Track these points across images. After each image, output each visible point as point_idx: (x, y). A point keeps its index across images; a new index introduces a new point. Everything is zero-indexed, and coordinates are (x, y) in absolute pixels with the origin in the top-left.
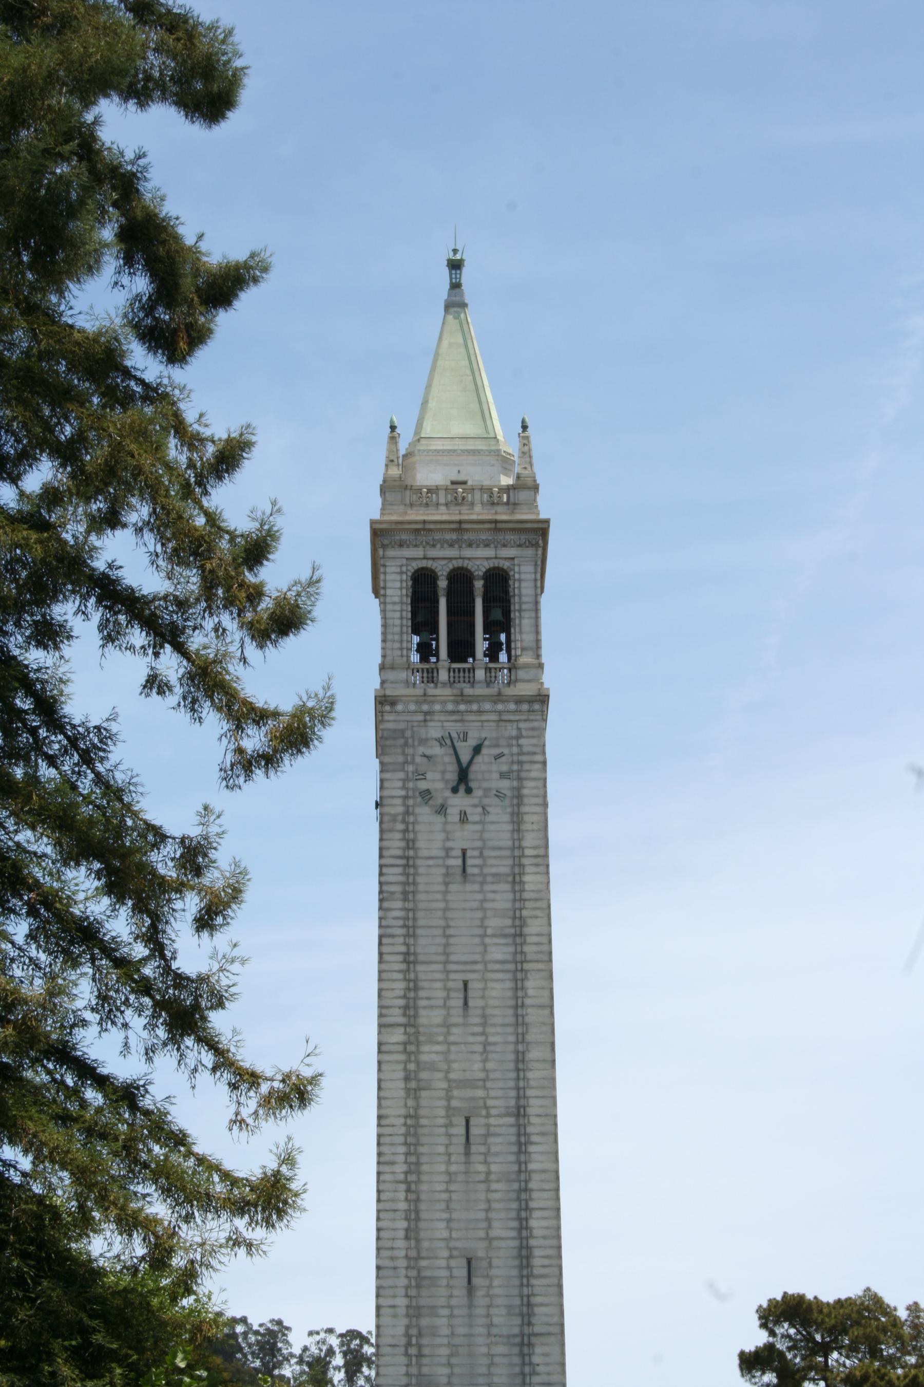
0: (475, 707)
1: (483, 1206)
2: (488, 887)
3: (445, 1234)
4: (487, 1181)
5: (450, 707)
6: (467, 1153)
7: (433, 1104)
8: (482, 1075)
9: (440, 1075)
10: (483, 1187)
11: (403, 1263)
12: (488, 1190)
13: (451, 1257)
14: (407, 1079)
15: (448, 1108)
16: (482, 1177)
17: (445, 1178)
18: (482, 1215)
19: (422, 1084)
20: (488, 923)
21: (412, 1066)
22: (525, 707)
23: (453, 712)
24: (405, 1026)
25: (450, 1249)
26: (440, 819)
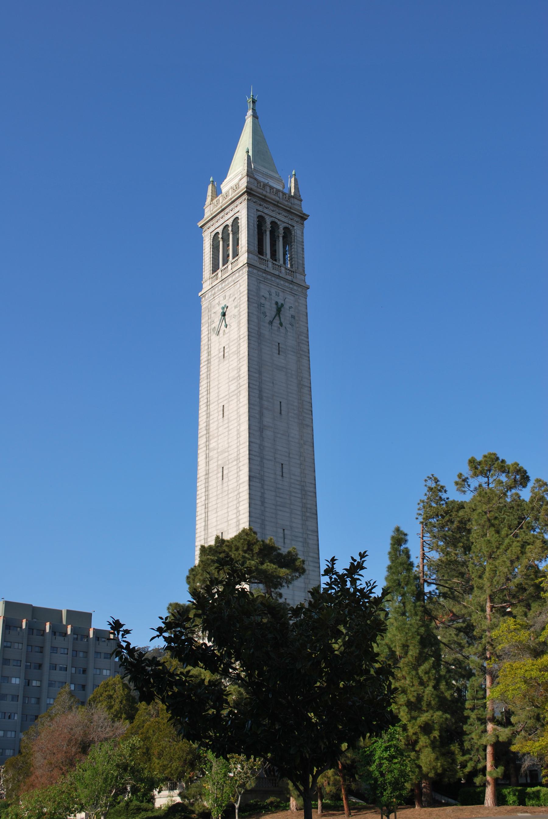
1: (226, 506)
2: (231, 360)
4: (228, 494)
5: (220, 287)
6: (222, 484)
8: (227, 446)
15: (218, 465)
16: (226, 493)
18: (226, 511)
20: (230, 376)
25: (217, 530)
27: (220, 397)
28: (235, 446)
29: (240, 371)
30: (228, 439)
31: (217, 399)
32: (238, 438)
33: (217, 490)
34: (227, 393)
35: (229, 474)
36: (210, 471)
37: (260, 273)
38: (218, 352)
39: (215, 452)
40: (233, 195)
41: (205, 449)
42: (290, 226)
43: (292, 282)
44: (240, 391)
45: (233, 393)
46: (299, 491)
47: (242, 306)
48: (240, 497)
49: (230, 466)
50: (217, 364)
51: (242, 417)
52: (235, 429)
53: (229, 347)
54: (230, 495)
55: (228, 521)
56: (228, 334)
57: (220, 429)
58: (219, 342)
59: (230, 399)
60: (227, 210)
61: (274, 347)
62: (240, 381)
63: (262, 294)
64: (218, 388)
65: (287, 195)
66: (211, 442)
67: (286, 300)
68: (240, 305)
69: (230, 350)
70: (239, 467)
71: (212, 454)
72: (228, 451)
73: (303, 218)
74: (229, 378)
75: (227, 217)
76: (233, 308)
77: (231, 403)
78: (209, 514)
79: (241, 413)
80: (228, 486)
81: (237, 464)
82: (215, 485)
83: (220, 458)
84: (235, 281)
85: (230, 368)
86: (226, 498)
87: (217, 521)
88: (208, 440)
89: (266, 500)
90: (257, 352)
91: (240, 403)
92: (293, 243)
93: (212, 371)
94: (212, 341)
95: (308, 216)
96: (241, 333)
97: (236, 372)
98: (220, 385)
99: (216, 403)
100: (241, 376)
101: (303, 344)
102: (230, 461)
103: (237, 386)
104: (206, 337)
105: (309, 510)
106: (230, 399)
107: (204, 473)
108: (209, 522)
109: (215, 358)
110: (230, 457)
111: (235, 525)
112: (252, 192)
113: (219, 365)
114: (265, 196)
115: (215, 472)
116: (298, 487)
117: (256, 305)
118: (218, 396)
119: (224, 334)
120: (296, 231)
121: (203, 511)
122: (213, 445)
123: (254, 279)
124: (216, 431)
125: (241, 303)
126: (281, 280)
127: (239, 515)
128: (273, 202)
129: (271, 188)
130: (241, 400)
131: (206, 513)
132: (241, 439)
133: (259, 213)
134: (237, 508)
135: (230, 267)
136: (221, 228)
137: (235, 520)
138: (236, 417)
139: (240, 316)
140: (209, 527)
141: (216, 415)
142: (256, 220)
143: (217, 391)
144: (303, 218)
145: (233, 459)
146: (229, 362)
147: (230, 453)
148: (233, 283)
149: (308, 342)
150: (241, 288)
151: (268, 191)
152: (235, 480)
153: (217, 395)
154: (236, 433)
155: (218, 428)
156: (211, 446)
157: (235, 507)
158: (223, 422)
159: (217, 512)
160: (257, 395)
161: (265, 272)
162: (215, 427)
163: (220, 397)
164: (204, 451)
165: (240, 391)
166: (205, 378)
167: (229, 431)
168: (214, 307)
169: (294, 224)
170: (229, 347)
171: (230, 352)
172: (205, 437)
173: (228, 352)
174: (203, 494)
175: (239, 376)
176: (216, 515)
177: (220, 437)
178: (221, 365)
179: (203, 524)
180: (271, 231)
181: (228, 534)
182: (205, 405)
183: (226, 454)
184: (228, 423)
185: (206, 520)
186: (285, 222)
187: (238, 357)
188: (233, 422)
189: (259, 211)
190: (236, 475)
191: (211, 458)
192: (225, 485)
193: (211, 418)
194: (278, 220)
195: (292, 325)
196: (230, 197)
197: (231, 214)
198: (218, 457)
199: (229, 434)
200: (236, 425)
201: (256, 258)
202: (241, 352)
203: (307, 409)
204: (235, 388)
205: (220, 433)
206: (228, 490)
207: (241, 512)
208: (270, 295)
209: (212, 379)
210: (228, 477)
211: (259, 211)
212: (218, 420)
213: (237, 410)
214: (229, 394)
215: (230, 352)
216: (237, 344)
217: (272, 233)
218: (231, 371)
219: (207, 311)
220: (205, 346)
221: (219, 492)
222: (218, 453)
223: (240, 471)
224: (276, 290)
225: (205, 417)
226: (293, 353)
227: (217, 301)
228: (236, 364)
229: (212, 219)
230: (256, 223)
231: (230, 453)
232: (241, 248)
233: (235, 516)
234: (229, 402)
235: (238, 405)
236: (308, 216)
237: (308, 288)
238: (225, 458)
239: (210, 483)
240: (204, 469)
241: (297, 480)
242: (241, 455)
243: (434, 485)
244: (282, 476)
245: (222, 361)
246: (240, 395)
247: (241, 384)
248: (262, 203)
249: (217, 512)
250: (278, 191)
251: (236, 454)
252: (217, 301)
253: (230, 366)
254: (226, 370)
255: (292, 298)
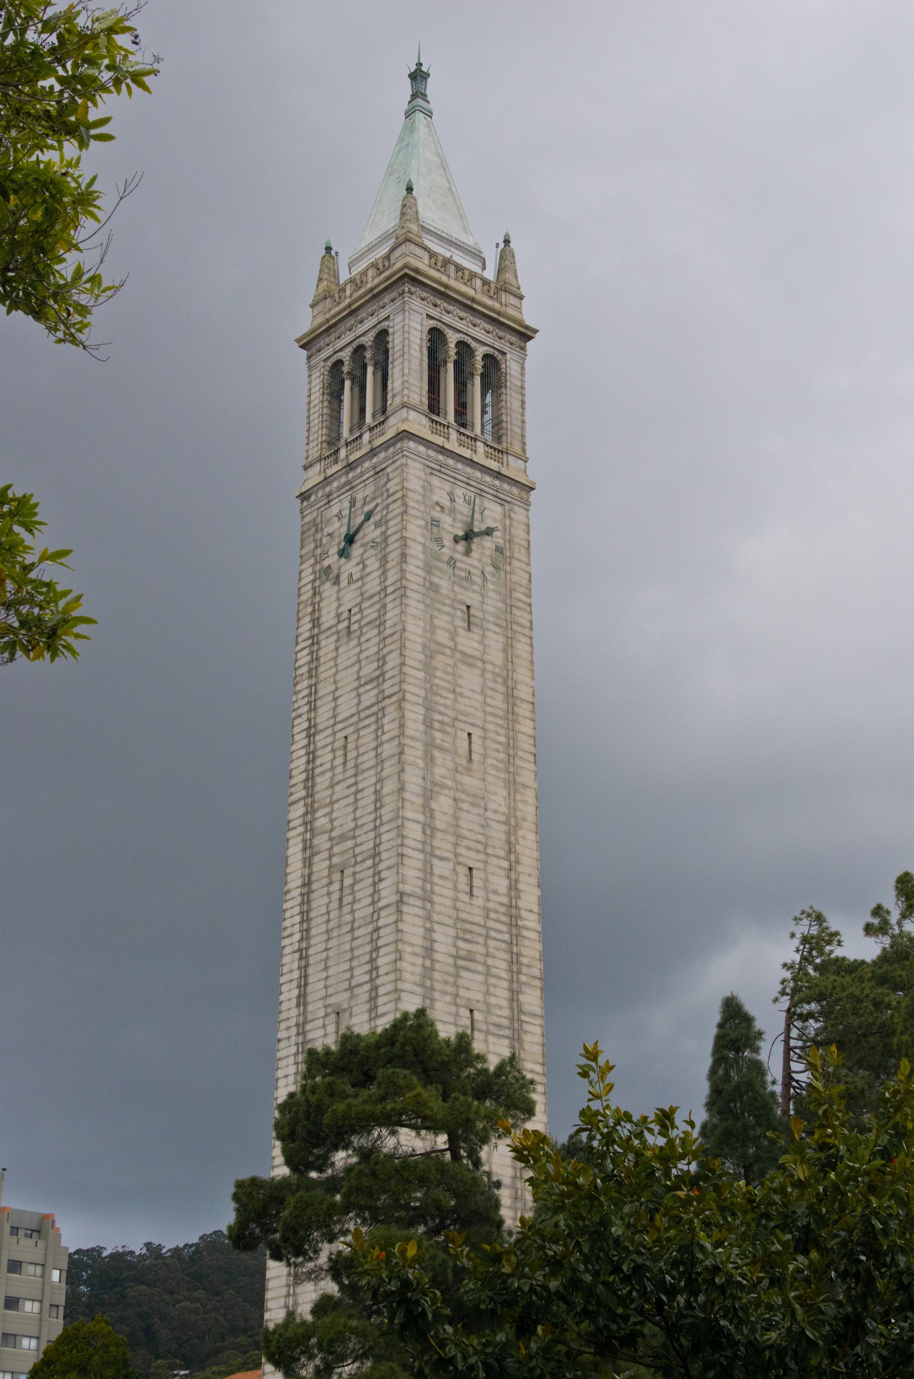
0: (359, 470)
1: (349, 956)
2: (363, 639)
3: (323, 993)
4: (352, 930)
5: (343, 480)
6: (341, 907)
7: (320, 866)
8: (352, 825)
9: (326, 836)
10: (348, 937)
11: (294, 1031)
12: (353, 939)
13: (326, 1015)
14: (304, 849)
15: (330, 867)
16: (348, 927)
17: (325, 937)
18: (347, 966)
19: (315, 850)
20: (362, 673)
21: (308, 836)
22: (391, 450)
23: (345, 485)
24: (304, 798)
25: (326, 1007)
26: (336, 588)
27: (339, 718)
28: (371, 826)
29: (384, 664)
30: (355, 811)
31: (331, 722)
32: (376, 809)
33: (328, 921)
34: (354, 710)
35: (356, 888)
36: (314, 878)
37: (432, 453)
38: (335, 621)
39: (326, 836)
40: (377, 281)
41: (301, 829)
42: (496, 353)
43: (498, 475)
44: (383, 708)
45: (368, 712)
46: (504, 928)
47: (391, 523)
48: (379, 938)
49: (358, 868)
50: (333, 647)
51: (387, 764)
52: (372, 789)
53: (361, 611)
54: (357, 933)
55: (351, 988)
56: (359, 583)
57: (338, 788)
58: (338, 599)
59: (361, 724)
60: (362, 314)
61: (459, 613)
62: (386, 685)
63: (435, 498)
64: (335, 699)
65: (493, 285)
66: (318, 814)
67: (486, 512)
68: (387, 522)
69: (362, 618)
70: (379, 872)
71: (322, 842)
72: (354, 837)
73: (525, 335)
74: (359, 678)
75: (361, 329)
76: (372, 527)
77: (362, 733)
78: (310, 970)
79: (384, 755)
80: (352, 912)
81: (374, 865)
82: (323, 910)
83: (336, 850)
84: (378, 469)
85: (363, 656)
86: (348, 937)
87: (326, 987)
88: (310, 811)
89: (436, 946)
90: (421, 623)
91: (383, 733)
92: (503, 390)
93: (322, 660)
94: (325, 595)
95: (536, 331)
96: (389, 582)
97: (375, 665)
98: (338, 694)
99: (329, 731)
100: (387, 676)
101: (518, 608)
102: (359, 859)
103: (377, 696)
104: (309, 586)
105: (524, 970)
106: (361, 724)
107: (299, 882)
108: (310, 989)
109: (328, 633)
110: (357, 850)
111: (366, 997)
112: (418, 277)
113: (337, 649)
114: (446, 286)
115: (325, 881)
116: (504, 919)
117: (422, 523)
118: (334, 716)
119: (349, 583)
120: (511, 364)
121: (295, 965)
122: (321, 822)
123: (420, 466)
124: (329, 792)
125: (389, 516)
126: (476, 469)
127: (378, 977)
128: (461, 299)
129: (459, 268)
130: (386, 728)
131: (304, 969)
132: (383, 811)
133: (433, 323)
134: (372, 961)
135: (366, 437)
136: (349, 350)
137: (367, 987)
138: (373, 762)
139: (387, 545)
140: (309, 999)
141: (330, 756)
142: (425, 337)
143: (333, 704)
144: (525, 335)
145: (365, 855)
146: (359, 644)
147: (359, 840)
148: (372, 473)
149: (530, 605)
150: (390, 485)
151: (452, 275)
152: (369, 900)
153: (331, 714)
154: (372, 798)
155: (332, 786)
156: (317, 824)
157: (367, 958)
158: (344, 772)
159: (326, 968)
160: (421, 718)
161: (442, 450)
162: (327, 784)
163: (339, 718)
164: (299, 835)
165: (383, 708)
166: (306, 675)
167: (357, 792)
168: (329, 522)
169: (506, 349)
170: (361, 611)
171: (363, 623)
172: (302, 803)
173: (359, 621)
174: (297, 927)
175: (383, 674)
176: (324, 975)
177: (336, 806)
178: (341, 650)
179: (296, 992)
180: (455, 362)
181: (351, 1016)
182: (304, 734)
183: (350, 843)
184: (355, 775)
185: (303, 983)
186: (485, 344)
187: (379, 634)
188: (366, 775)
189: (432, 318)
190: (371, 890)
191: (315, 850)
192: (346, 909)
193: (318, 762)
194: (473, 338)
195: (497, 568)
196: (369, 286)
197: (372, 321)
198: (330, 849)
199: (356, 801)
200: (373, 780)
201: (425, 421)
202: (388, 624)
203: (525, 751)
204: (373, 700)
205: (335, 797)
206: (353, 921)
207: (382, 971)
208: (452, 500)
209: (322, 677)
210: (353, 892)
211: (432, 318)
212: (332, 768)
213: (376, 748)
214: (359, 712)
215: (363, 623)
216: (377, 607)
217: (458, 365)
218: (363, 663)
219: (313, 529)
220: (306, 606)
221: (332, 925)
222: (331, 839)
223: (380, 880)
224: (465, 491)
225: (304, 759)
226: (498, 629)
227: (335, 510)
228: (375, 649)
229: (328, 330)
230: (425, 344)
231: (359, 840)
232: (394, 396)
233: (367, 977)
234: (358, 730)
235: (377, 737)
236: (536, 331)
237: (533, 489)
238: (346, 851)
239: (314, 905)
240: (299, 873)
241: (502, 904)
242: (383, 848)
243: (814, 931)
244: (471, 895)
245: (345, 639)
246: (384, 715)
247: (387, 693)
248: (438, 302)
249: (326, 968)
250: (473, 275)
251: (371, 844)
252: (335, 510)
253: (361, 652)
254: (354, 659)
255: (499, 509)
